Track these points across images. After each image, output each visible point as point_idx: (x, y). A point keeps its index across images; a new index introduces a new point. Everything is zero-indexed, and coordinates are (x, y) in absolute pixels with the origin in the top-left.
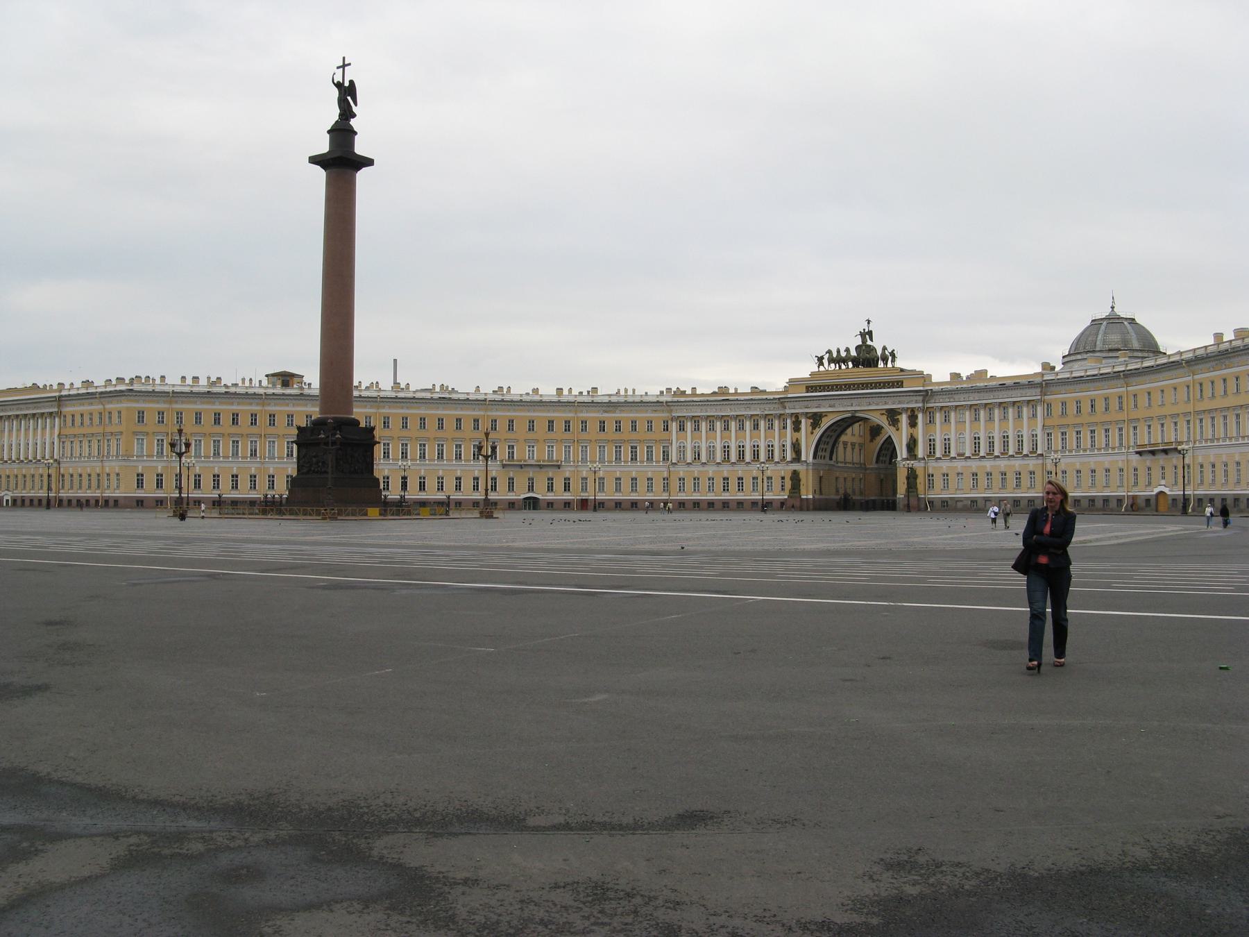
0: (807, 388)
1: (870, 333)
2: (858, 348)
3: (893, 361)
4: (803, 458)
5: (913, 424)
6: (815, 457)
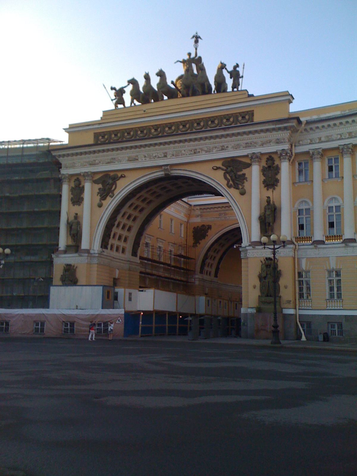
0: (96, 136)
1: (198, 61)
3: (236, 85)
4: (85, 245)
6: (104, 244)
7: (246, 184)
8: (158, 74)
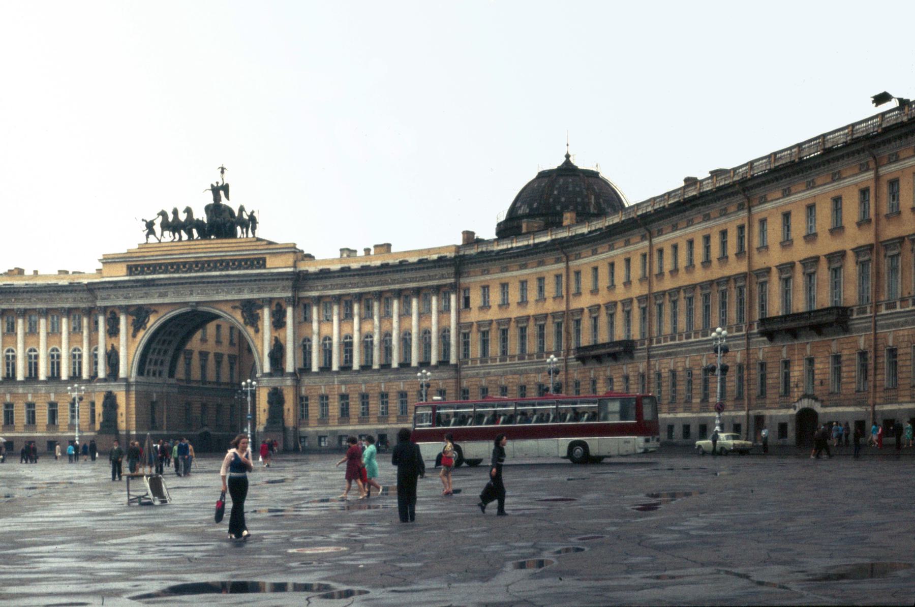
2: (208, 209)
4: (122, 373)
5: (278, 323)
6: (140, 372)
7: (259, 323)
8: (184, 212)
